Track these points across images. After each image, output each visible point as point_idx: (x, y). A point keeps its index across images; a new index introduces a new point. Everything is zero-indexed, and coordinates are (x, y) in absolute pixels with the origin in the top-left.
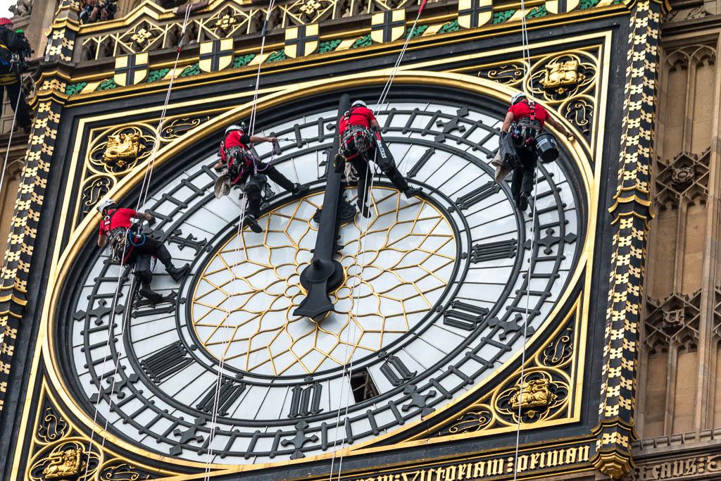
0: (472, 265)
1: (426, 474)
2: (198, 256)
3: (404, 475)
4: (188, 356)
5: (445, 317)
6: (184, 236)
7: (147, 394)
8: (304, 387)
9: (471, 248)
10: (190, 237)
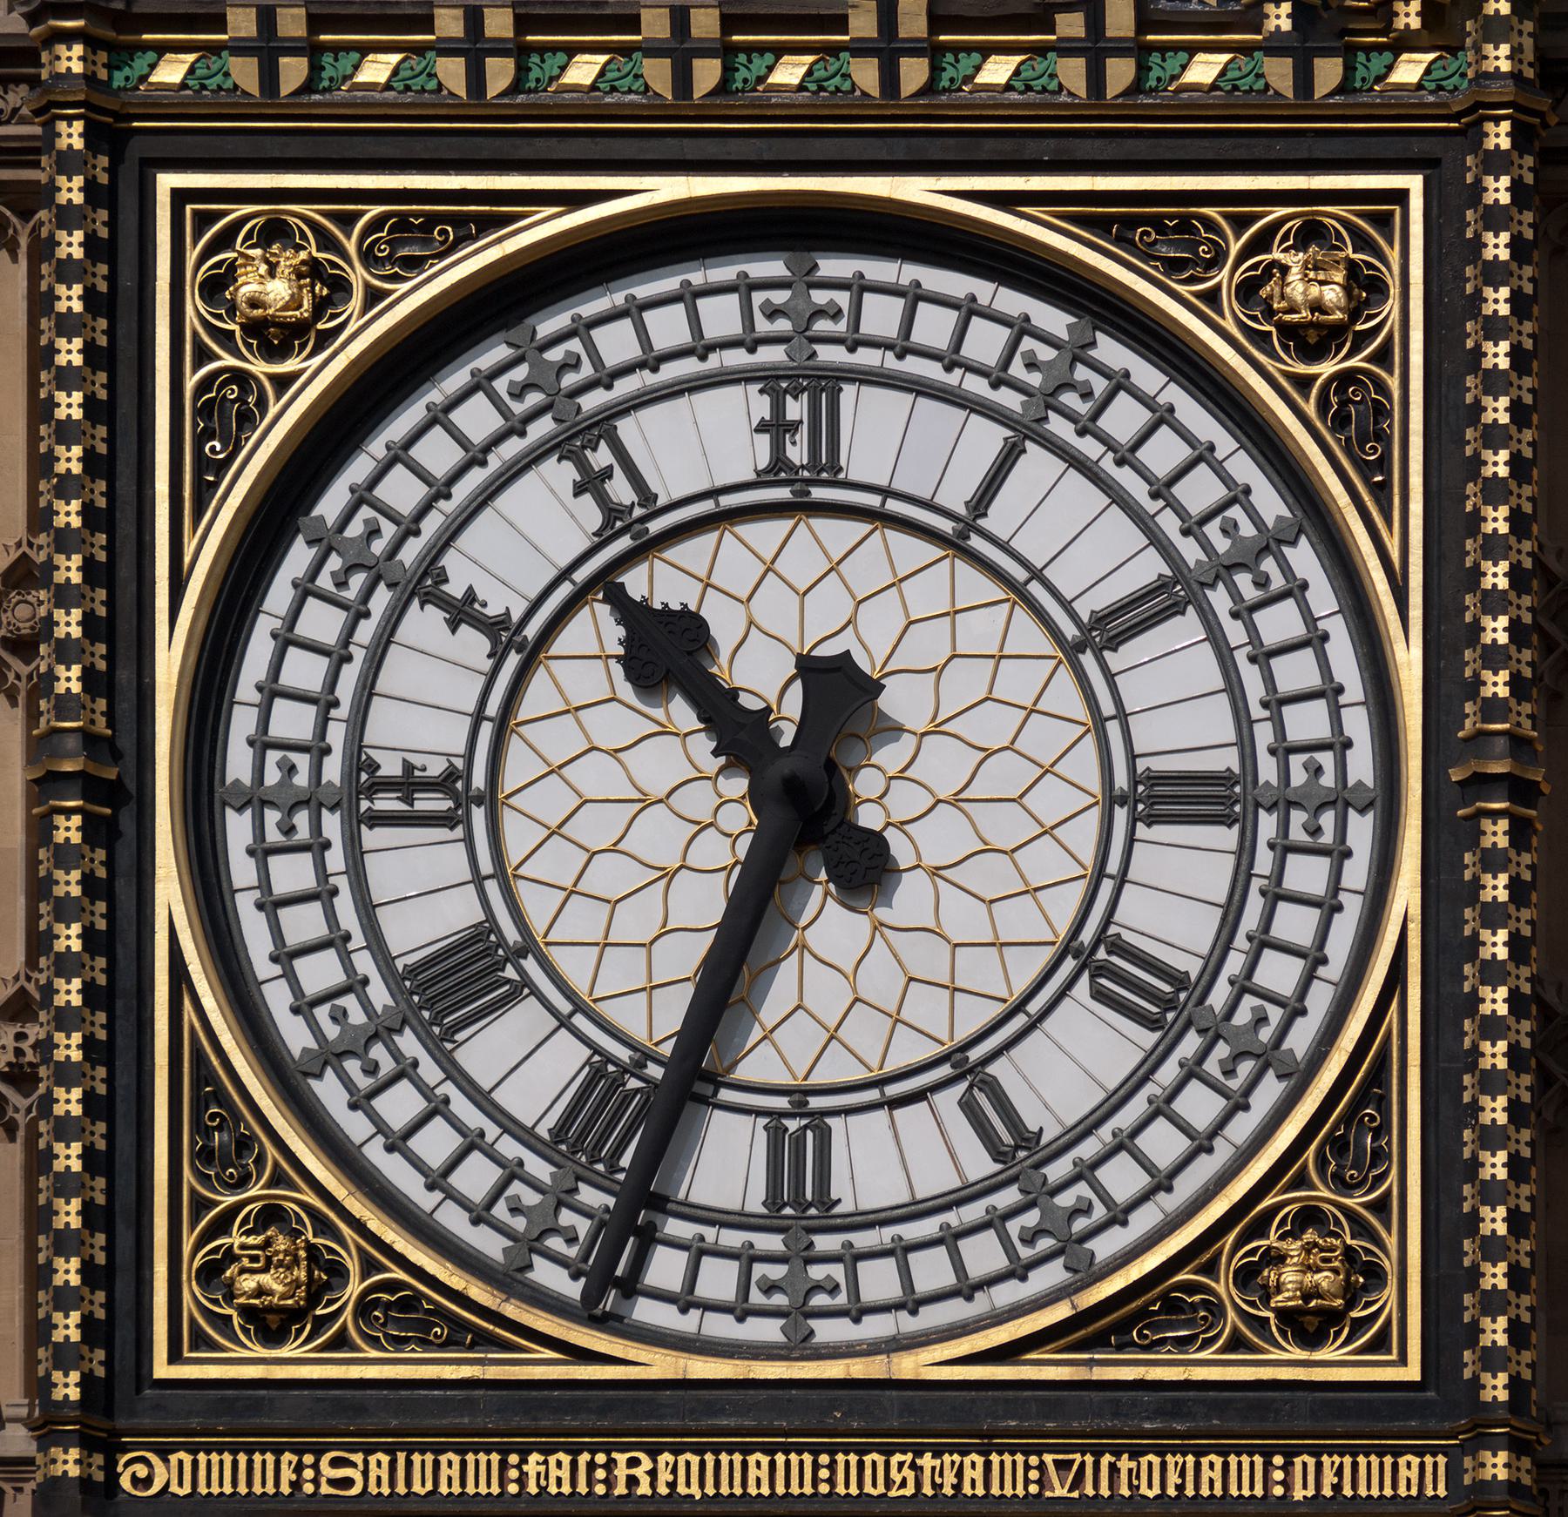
0: (1142, 831)
1: (1097, 1465)
2: (498, 656)
3: (1048, 1458)
4: (510, 972)
5: (1092, 977)
6: (455, 589)
7: (430, 1071)
8: (793, 1125)
9: (1134, 780)
10: (471, 596)
